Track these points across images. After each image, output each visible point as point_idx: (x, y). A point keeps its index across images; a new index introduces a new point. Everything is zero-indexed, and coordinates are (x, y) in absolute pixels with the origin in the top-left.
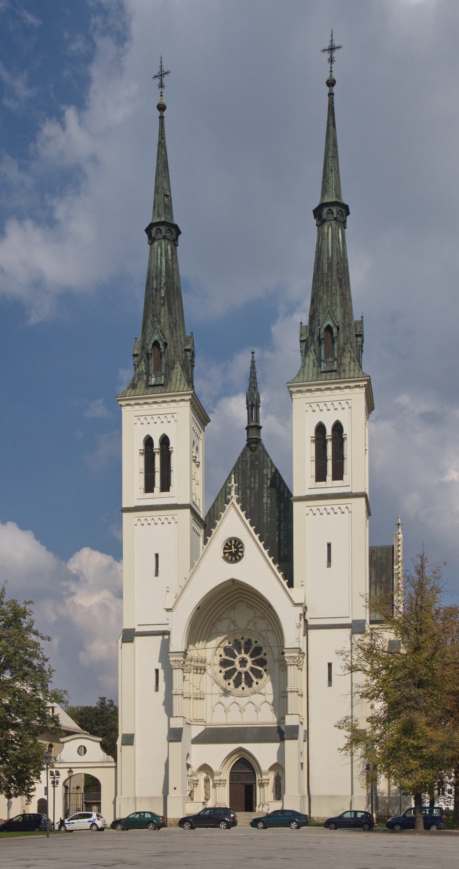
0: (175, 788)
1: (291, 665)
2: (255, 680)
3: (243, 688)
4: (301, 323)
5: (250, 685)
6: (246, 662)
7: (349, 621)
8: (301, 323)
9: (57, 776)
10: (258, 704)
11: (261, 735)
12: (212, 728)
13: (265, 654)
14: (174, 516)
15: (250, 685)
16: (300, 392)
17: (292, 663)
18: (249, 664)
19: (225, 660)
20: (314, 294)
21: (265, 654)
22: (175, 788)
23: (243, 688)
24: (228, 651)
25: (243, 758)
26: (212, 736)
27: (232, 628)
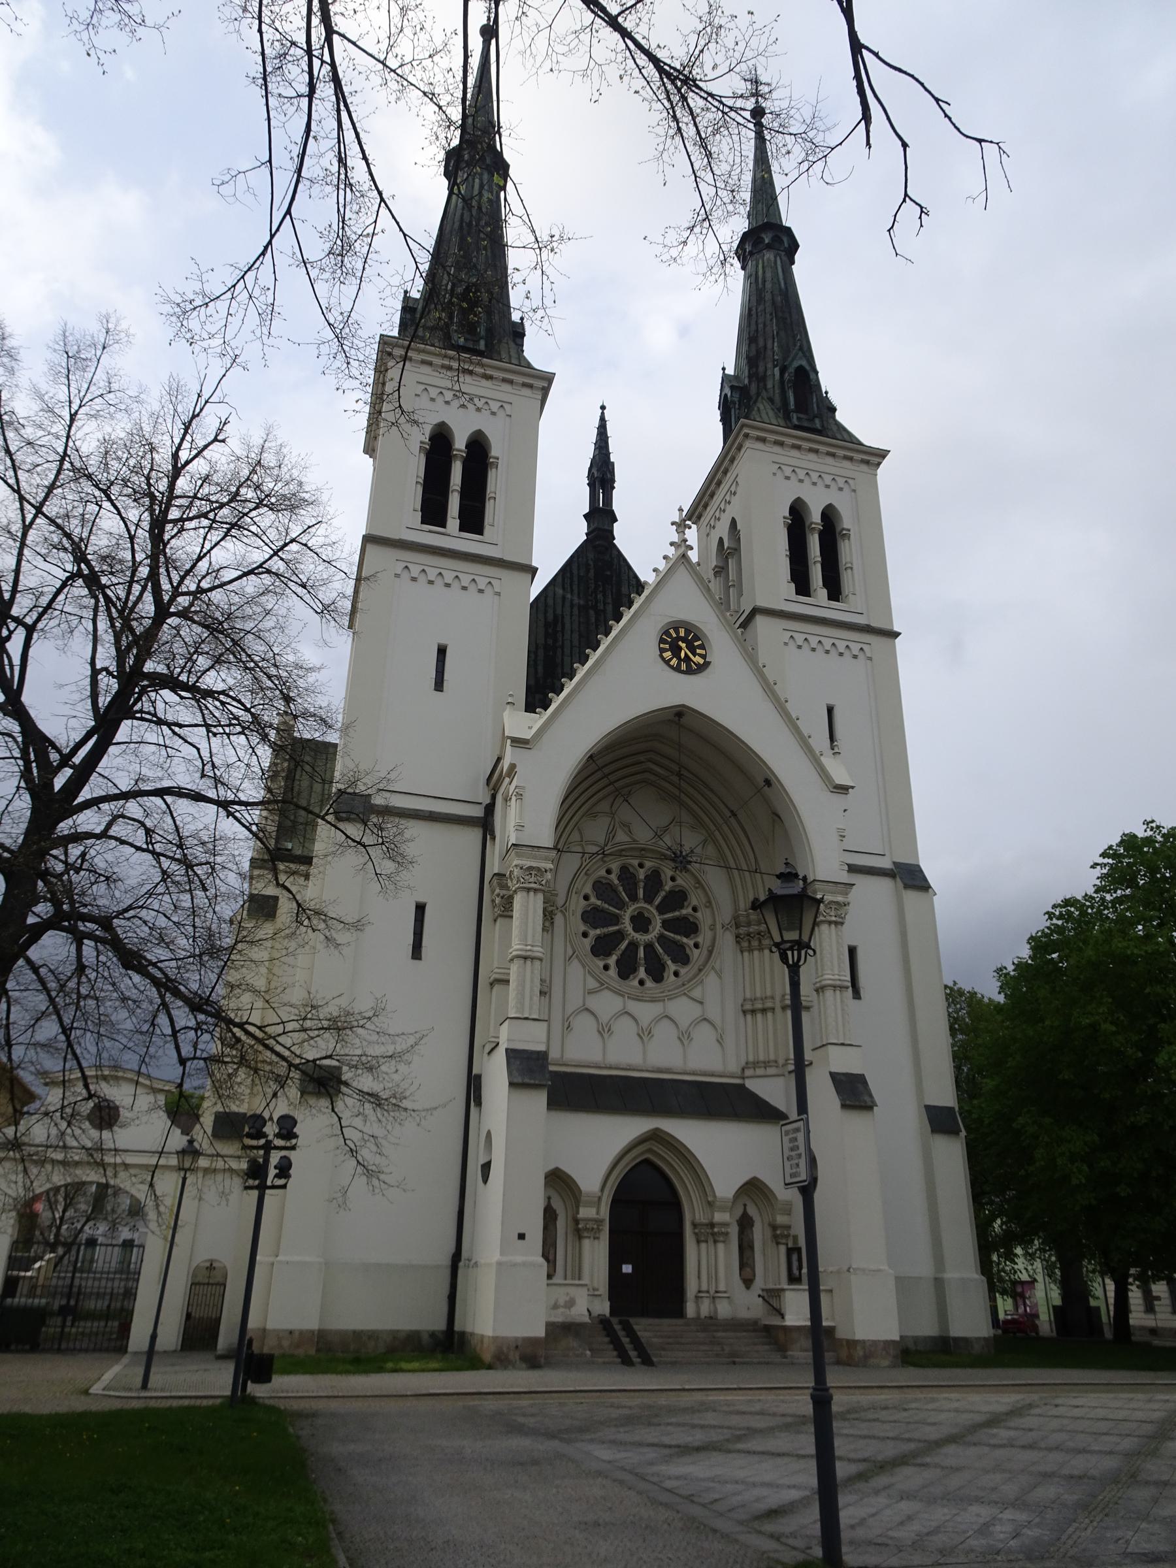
0: (522, 1236)
1: (830, 923)
2: (672, 967)
3: (642, 983)
4: (724, 369)
5: (658, 977)
6: (648, 922)
7: (885, 863)
8: (724, 369)
9: (279, 1142)
10: (684, 1023)
11: (727, 1101)
12: (566, 1074)
13: (695, 909)
14: (493, 581)
15: (658, 977)
16: (759, 439)
17: (834, 919)
18: (657, 928)
19: (596, 909)
20: (757, 331)
21: (695, 909)
22: (522, 1236)
23: (642, 983)
24: (602, 888)
25: (647, 1162)
26: (577, 1092)
27: (621, 837)
